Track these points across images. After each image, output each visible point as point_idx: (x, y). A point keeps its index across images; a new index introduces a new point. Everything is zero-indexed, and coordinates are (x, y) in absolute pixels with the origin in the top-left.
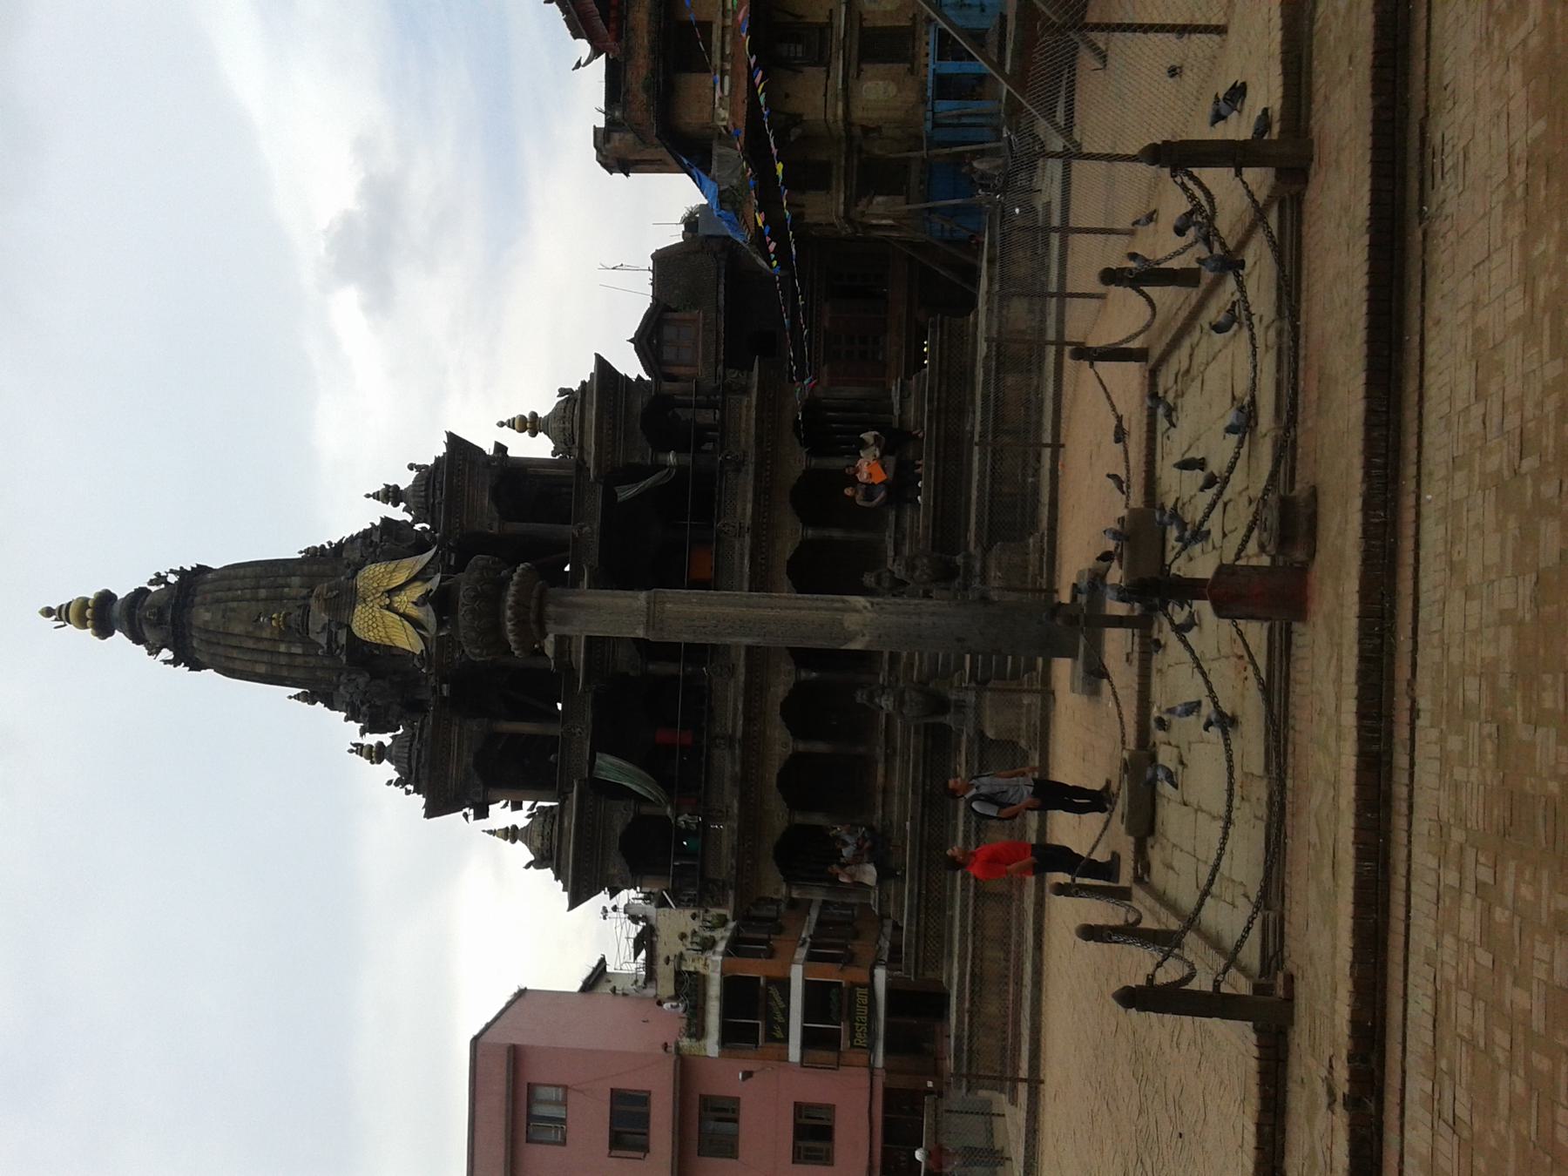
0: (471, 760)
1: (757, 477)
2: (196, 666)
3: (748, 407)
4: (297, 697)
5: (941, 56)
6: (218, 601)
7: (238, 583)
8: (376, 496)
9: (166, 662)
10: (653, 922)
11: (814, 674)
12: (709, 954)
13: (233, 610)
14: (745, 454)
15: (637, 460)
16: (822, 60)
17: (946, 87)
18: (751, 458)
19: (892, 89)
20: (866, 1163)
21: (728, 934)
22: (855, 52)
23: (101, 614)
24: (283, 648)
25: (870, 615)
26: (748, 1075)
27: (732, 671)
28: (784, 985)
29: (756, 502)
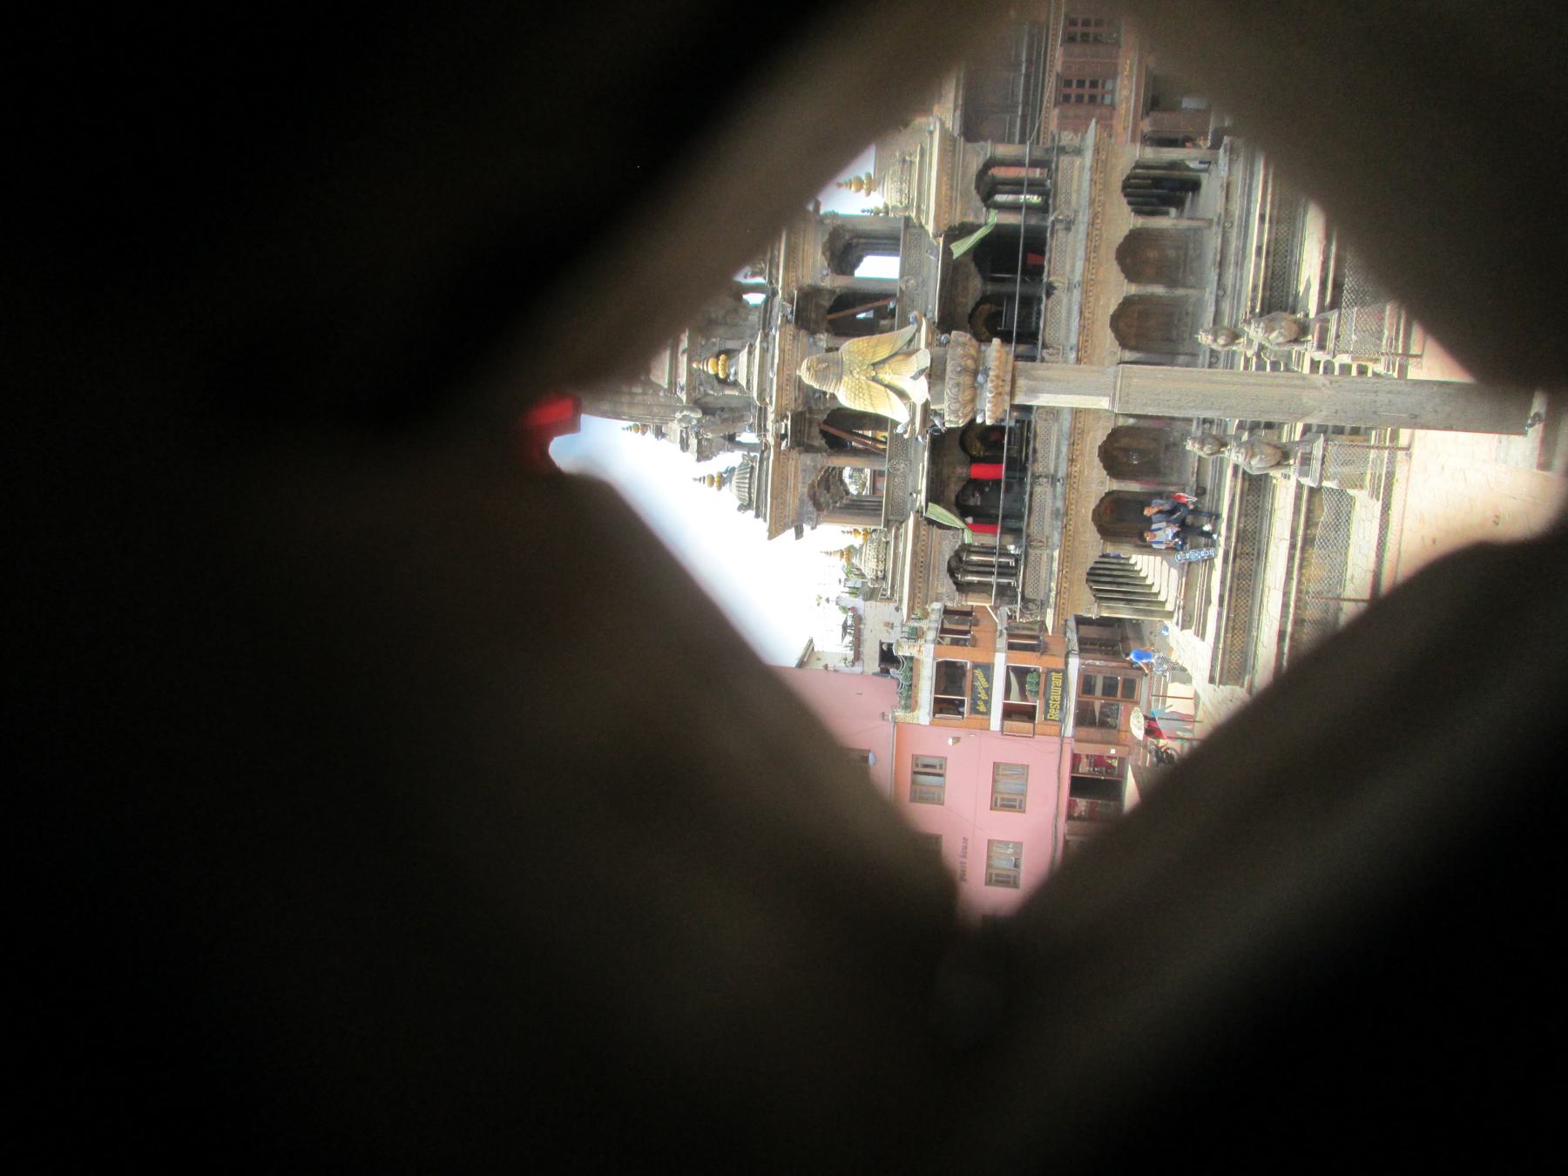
3: (1082, 168)
10: (861, 612)
12: (921, 642)
14: (1076, 212)
15: (970, 219)
20: (1053, 810)
21: (935, 625)
26: (957, 740)
28: (988, 669)
29: (1087, 259)
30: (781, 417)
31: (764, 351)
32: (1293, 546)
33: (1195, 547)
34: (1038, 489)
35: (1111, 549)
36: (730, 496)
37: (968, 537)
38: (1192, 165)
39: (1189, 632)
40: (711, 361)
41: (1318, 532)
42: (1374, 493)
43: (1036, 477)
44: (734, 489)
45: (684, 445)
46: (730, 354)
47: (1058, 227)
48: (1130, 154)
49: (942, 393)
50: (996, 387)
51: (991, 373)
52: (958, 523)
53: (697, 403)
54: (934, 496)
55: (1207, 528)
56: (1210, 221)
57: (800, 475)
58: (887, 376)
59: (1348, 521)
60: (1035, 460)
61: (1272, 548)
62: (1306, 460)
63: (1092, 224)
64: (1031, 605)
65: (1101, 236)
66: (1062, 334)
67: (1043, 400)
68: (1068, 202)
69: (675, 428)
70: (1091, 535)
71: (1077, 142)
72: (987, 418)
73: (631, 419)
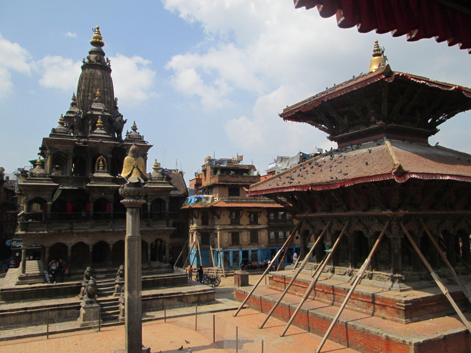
0: (61, 150)
1: (146, 231)
2: (83, 68)
3: (163, 227)
4: (74, 95)
5: (234, 252)
6: (103, 77)
7: (108, 83)
8: (135, 124)
9: (84, 60)
11: (91, 250)
13: (101, 81)
14: (152, 227)
16: (232, 223)
17: (226, 254)
18: (150, 229)
19: (226, 241)
22: (234, 231)
23: (98, 43)
25: (137, 297)
27: (92, 227)
30: (85, 143)
31: (106, 138)
32: (58, 305)
34: (68, 225)
35: (47, 249)
36: (57, 126)
37: (49, 203)
38: (164, 257)
39: (18, 280)
40: (101, 122)
41: (64, 311)
42: (82, 325)
44: (59, 127)
45: (69, 112)
47: (148, 222)
48: (167, 240)
50: (134, 202)
51: (138, 201)
52: (54, 200)
53: (86, 117)
58: (135, 171)
59: (67, 321)
61: (54, 300)
62: (91, 302)
63: (149, 231)
67: (129, 217)
69: (76, 110)
71: (170, 225)
73: (78, 95)
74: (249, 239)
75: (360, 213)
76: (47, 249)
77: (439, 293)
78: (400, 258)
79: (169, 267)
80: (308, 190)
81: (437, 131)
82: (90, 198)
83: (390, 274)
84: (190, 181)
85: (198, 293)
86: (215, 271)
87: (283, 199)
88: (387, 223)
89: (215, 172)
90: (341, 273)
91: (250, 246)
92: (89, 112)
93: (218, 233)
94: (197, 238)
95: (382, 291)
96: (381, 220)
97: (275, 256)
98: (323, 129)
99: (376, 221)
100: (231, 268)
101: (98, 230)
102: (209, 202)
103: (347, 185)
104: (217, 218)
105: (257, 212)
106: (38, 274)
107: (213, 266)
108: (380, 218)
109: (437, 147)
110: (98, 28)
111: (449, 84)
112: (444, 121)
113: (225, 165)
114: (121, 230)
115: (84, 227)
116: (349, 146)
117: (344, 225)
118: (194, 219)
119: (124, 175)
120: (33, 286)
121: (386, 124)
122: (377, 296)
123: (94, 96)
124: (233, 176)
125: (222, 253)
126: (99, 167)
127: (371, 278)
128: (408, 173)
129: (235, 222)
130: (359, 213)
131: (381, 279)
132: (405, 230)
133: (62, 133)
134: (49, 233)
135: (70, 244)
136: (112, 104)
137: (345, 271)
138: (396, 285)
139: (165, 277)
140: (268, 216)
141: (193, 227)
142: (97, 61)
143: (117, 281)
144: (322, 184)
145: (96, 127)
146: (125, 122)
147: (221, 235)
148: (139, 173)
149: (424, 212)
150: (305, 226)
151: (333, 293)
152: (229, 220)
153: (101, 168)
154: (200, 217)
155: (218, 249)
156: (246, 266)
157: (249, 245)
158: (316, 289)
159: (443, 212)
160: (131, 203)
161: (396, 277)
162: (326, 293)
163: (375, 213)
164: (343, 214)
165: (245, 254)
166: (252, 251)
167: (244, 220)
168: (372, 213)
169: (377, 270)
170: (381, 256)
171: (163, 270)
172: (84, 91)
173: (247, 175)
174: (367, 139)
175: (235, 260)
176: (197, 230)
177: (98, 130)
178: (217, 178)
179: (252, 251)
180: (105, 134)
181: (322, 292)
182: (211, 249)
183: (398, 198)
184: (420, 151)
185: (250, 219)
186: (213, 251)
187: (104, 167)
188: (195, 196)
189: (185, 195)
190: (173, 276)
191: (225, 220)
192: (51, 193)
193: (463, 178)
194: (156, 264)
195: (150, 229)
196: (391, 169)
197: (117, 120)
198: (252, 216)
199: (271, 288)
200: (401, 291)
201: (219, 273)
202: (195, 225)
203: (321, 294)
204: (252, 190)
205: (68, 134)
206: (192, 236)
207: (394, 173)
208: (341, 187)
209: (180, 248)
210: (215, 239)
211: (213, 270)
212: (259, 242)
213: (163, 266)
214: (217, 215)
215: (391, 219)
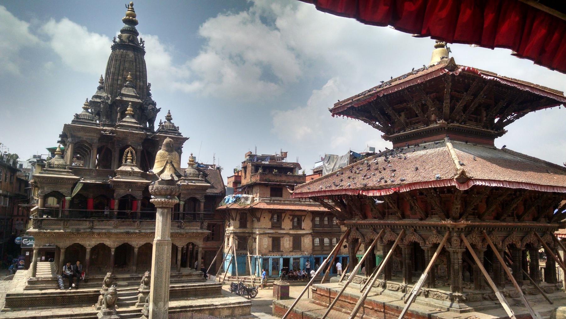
2: (113, 48)
3: (197, 229)
4: (102, 77)
5: (273, 259)
6: (136, 60)
8: (169, 113)
9: (115, 38)
11: (113, 253)
14: (183, 229)
16: (273, 227)
17: (265, 261)
18: (182, 231)
19: (266, 246)
23: (131, 21)
24: (120, 78)
27: (116, 227)
30: (112, 132)
31: (136, 128)
33: (64, 282)
34: (88, 223)
35: (62, 251)
36: (80, 111)
37: (68, 198)
39: (27, 284)
40: (132, 109)
43: (93, 222)
46: (133, 116)
48: (200, 243)
49: (163, 184)
50: (165, 202)
52: (74, 195)
53: (115, 103)
54: (85, 185)
55: (73, 285)
56: (179, 271)
57: (91, 138)
58: (168, 166)
60: (99, 221)
61: (68, 309)
62: (109, 314)
63: (180, 234)
64: (39, 223)
65: (176, 237)
66: (144, 227)
67: (159, 218)
68: (187, 226)
69: (104, 95)
70: (68, 243)
72: (153, 199)
74: (291, 245)
75: (416, 221)
76: (62, 251)
77: (504, 316)
78: (461, 274)
79: (201, 275)
80: (359, 194)
81: (504, 132)
82: (115, 195)
83: (448, 293)
84: (228, 178)
85: (232, 306)
86: (252, 281)
87: (330, 202)
88: (446, 235)
89: (256, 170)
90: (394, 289)
91: (291, 253)
92: (118, 98)
93: (257, 237)
94: (234, 242)
95: (440, 312)
96: (440, 230)
97: (319, 265)
98: (377, 127)
99: (434, 232)
100: (270, 277)
101: (122, 231)
102: (249, 202)
103: (403, 190)
104: (256, 221)
105: (301, 216)
106: (51, 278)
107: (249, 275)
108: (439, 228)
109: (504, 150)
110: (132, 5)
111: (518, 80)
112: (513, 121)
113: (267, 163)
114: (148, 231)
115: (106, 227)
116: (405, 146)
117: (398, 234)
118: (231, 221)
119: (156, 169)
120: (43, 291)
121: (448, 123)
122: (434, 316)
123: (125, 80)
124: (276, 175)
125: (260, 261)
126: (126, 160)
127: (427, 296)
128: (471, 179)
129: (277, 225)
130: (415, 222)
131: (439, 297)
132: (467, 243)
133: (87, 119)
134: (65, 232)
135: (89, 245)
136: (144, 90)
137: (398, 286)
138: (456, 305)
139: (196, 286)
140: (313, 220)
141: (230, 229)
142: (130, 41)
143: (141, 290)
144: (375, 188)
145: (126, 115)
146: (159, 110)
147: (260, 239)
148: (172, 169)
149: (488, 223)
150: (353, 234)
151: (384, 312)
152: (270, 223)
153: (128, 161)
154: (238, 218)
155: (257, 255)
156: (287, 276)
157: (291, 252)
158: (365, 305)
159: (510, 224)
160: (162, 203)
161: (455, 296)
162: (376, 311)
163: (433, 223)
164: (397, 222)
165: (286, 261)
166: (294, 259)
167: (287, 224)
168: (430, 223)
169: (435, 287)
170: (439, 272)
171: (194, 278)
172: (114, 74)
173: (291, 174)
174: (426, 139)
175: (275, 268)
176: (234, 233)
177: (127, 119)
178: (259, 177)
179: (294, 259)
180: (135, 123)
181: (372, 309)
182: (249, 255)
183: (459, 206)
184: (485, 154)
185: (293, 223)
186: (251, 257)
187: (132, 160)
188: (234, 195)
189: (222, 194)
190: (205, 285)
191: (265, 223)
192: (71, 186)
193: (533, 187)
194: (186, 271)
195: (182, 231)
196: (453, 175)
197: (150, 107)
198: (296, 220)
199: (314, 303)
200: (462, 312)
201: (258, 282)
202: (232, 228)
203: (371, 312)
204: (298, 191)
205: (93, 121)
206: (228, 239)
207: (457, 179)
208: (395, 192)
209: (213, 253)
210: (254, 244)
211: (250, 279)
212: (303, 249)
213: (194, 273)
214: (256, 218)
215: (451, 230)
